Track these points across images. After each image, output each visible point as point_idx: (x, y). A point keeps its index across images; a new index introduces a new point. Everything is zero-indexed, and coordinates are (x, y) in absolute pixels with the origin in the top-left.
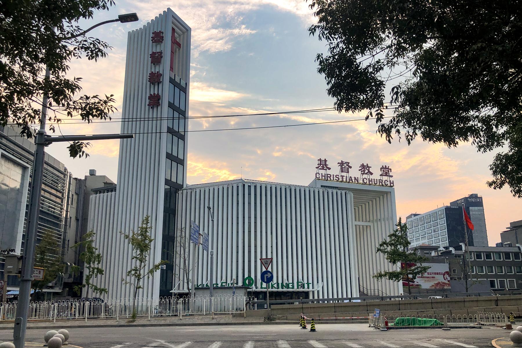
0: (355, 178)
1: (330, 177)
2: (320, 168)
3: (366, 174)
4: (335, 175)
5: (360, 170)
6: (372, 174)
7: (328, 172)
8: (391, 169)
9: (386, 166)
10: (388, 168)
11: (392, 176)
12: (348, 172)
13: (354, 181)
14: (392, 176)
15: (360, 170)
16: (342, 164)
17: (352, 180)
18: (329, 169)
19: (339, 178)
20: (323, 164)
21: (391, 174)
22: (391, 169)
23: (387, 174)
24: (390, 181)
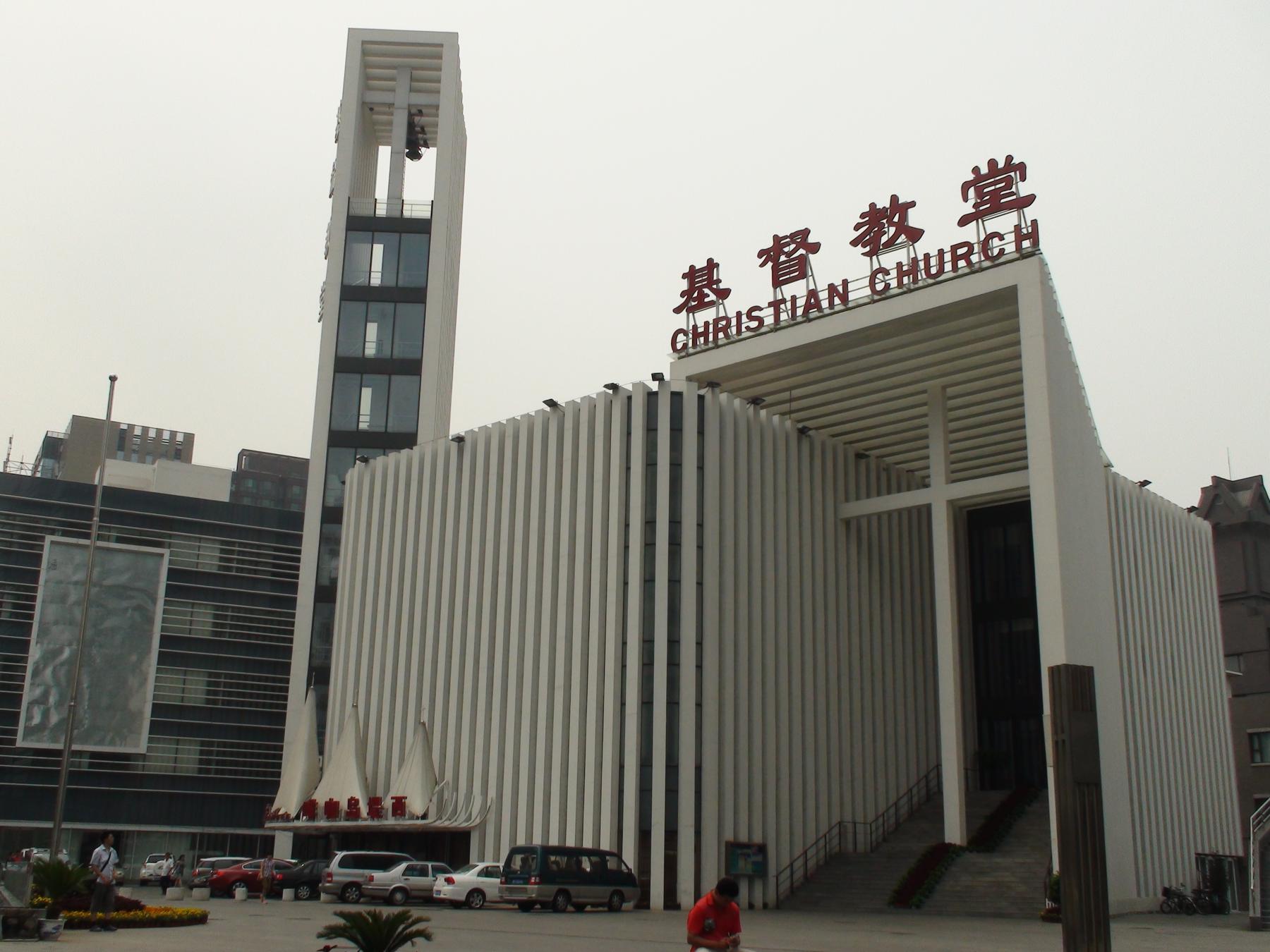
0: (832, 288)
3: (891, 244)
4: (744, 311)
5: (854, 243)
9: (992, 163)
11: (1030, 199)
13: (825, 304)
14: (1030, 199)
15: (854, 243)
17: (818, 305)
18: (724, 294)
19: (761, 320)
20: (702, 284)
21: (1024, 189)
22: (1022, 168)
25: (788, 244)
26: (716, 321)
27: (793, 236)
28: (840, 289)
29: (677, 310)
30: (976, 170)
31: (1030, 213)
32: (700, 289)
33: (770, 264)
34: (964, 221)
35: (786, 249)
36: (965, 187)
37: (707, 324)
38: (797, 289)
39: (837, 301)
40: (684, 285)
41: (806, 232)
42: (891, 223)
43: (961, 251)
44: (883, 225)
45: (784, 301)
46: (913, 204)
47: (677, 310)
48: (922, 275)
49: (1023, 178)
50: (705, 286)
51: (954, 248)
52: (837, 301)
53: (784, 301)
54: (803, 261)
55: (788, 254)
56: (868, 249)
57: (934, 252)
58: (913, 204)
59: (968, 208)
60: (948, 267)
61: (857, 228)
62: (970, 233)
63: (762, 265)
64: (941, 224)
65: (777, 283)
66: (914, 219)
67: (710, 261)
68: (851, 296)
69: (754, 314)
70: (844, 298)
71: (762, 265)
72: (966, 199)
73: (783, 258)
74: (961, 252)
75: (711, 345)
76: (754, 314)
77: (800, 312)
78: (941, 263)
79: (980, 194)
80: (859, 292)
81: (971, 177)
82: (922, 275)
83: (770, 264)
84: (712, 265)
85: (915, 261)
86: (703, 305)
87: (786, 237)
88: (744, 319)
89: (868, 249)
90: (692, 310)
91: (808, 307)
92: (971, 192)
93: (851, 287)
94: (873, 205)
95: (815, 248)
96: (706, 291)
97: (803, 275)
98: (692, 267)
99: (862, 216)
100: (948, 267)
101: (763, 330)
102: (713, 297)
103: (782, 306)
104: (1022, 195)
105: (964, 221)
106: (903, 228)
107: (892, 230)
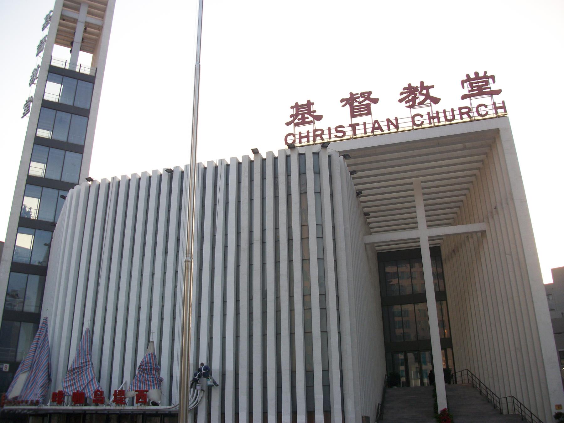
0: (389, 121)
1: (321, 135)
2: (296, 121)
3: (421, 103)
4: (333, 127)
5: (401, 101)
6: (436, 101)
7: (319, 125)
8: (493, 77)
9: (476, 74)
10: (485, 76)
11: (498, 92)
12: (369, 113)
13: (385, 128)
14: (498, 92)
15: (401, 101)
16: (350, 101)
17: (380, 128)
18: (319, 118)
20: (303, 112)
21: (493, 87)
22: (493, 77)
23: (480, 92)
24: (494, 104)
25: (359, 98)
26: (315, 131)
27: (362, 94)
28: (394, 122)
29: (288, 124)
30: (468, 76)
31: (498, 99)
32: (303, 115)
33: (348, 106)
34: (464, 97)
35: (358, 100)
36: (463, 82)
37: (308, 132)
38: (368, 119)
39: (392, 127)
40: (293, 111)
41: (370, 93)
42: (421, 93)
43: (463, 111)
44: (413, 94)
45: (358, 124)
46: (433, 87)
47: (288, 124)
48: (442, 119)
49: (494, 82)
50: (306, 113)
51: (460, 109)
52: (392, 127)
53: (358, 124)
54: (368, 105)
55: (360, 103)
56: (408, 104)
57: (448, 109)
58: (433, 87)
59: (466, 92)
60: (457, 117)
61: (402, 94)
62: (466, 103)
63: (343, 106)
64: (451, 97)
65: (353, 116)
66: (432, 93)
67: (309, 101)
68: (400, 126)
69: (339, 129)
70: (397, 126)
71: (343, 106)
72: (463, 87)
73: (356, 104)
74: (466, 111)
75: (311, 143)
76: (339, 129)
77: (368, 131)
78: (453, 115)
79: (471, 85)
80: (405, 125)
81: (465, 78)
82: (442, 119)
83: (348, 106)
84: (309, 104)
85: (437, 112)
86: (304, 122)
87: (358, 94)
88: (333, 131)
89: (408, 104)
90: (296, 125)
91: (374, 129)
92: (466, 85)
93: (399, 121)
94: (410, 85)
95: (376, 101)
96: (306, 116)
97: (369, 113)
98: (297, 104)
99: (404, 89)
100: (457, 117)
101: (345, 138)
102: (311, 119)
103: (357, 127)
104: (492, 89)
105: (464, 97)
106: (428, 96)
107: (422, 98)
